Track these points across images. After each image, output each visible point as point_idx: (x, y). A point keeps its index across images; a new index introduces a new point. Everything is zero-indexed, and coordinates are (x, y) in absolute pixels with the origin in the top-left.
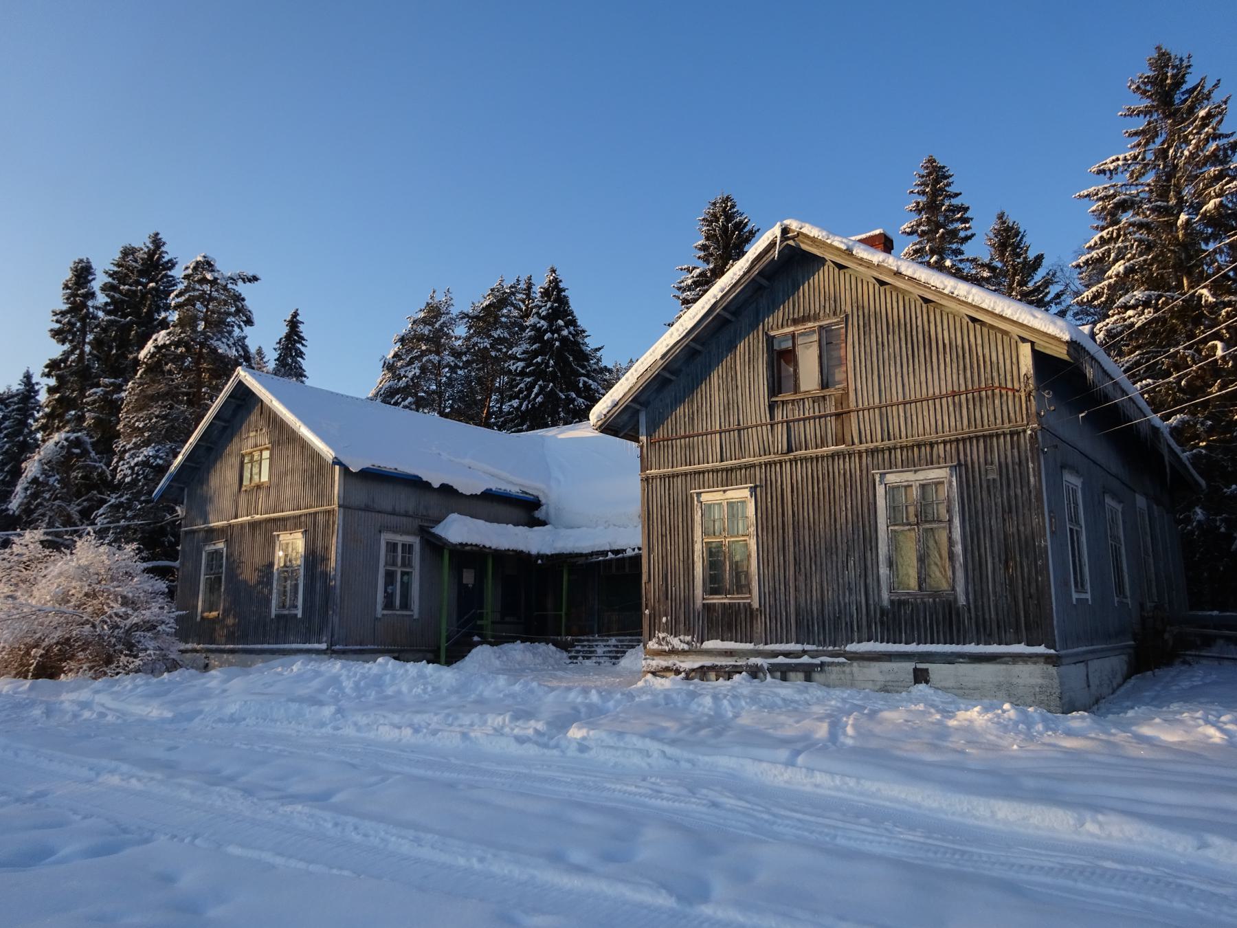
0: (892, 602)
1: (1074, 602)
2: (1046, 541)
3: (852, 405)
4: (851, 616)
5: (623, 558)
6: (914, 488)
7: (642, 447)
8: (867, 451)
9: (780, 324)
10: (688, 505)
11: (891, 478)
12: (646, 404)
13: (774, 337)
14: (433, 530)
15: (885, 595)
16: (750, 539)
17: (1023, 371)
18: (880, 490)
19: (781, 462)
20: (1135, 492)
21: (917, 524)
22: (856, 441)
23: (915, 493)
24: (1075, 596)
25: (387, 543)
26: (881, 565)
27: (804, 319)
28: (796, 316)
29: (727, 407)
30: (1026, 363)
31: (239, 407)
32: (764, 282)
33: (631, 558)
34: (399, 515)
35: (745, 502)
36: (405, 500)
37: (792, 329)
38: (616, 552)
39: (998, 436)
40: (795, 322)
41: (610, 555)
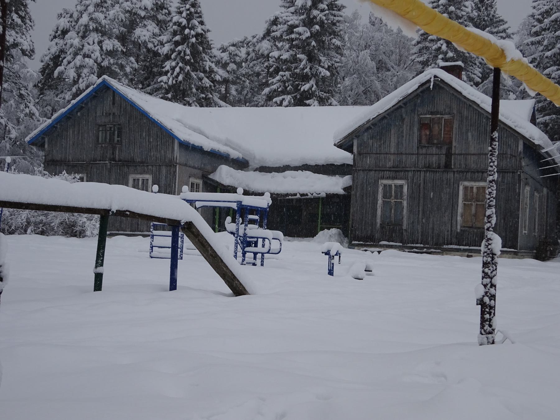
0: (461, 230)
1: (523, 234)
2: (519, 212)
3: (453, 153)
4: (445, 234)
5: (306, 199)
6: (474, 188)
7: (354, 156)
8: (457, 171)
9: (425, 112)
10: (376, 183)
11: (467, 183)
12: (358, 137)
13: (421, 118)
14: (211, 176)
15: (459, 227)
16: (404, 201)
17: (520, 150)
18: (461, 188)
19: (420, 171)
20: (544, 187)
21: (474, 202)
22: (453, 167)
23: (475, 190)
24: (524, 232)
25: (192, 183)
26: (458, 216)
27: (437, 113)
28: (433, 111)
29: (398, 144)
30: (521, 147)
31: (95, 97)
32: (421, 94)
33: (311, 199)
34: (195, 168)
35: (402, 185)
36: (195, 160)
37: (430, 116)
38: (302, 195)
39: (508, 172)
40: (432, 113)
41: (298, 196)
